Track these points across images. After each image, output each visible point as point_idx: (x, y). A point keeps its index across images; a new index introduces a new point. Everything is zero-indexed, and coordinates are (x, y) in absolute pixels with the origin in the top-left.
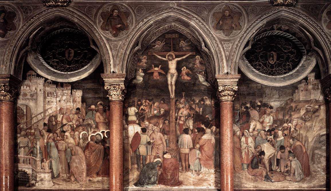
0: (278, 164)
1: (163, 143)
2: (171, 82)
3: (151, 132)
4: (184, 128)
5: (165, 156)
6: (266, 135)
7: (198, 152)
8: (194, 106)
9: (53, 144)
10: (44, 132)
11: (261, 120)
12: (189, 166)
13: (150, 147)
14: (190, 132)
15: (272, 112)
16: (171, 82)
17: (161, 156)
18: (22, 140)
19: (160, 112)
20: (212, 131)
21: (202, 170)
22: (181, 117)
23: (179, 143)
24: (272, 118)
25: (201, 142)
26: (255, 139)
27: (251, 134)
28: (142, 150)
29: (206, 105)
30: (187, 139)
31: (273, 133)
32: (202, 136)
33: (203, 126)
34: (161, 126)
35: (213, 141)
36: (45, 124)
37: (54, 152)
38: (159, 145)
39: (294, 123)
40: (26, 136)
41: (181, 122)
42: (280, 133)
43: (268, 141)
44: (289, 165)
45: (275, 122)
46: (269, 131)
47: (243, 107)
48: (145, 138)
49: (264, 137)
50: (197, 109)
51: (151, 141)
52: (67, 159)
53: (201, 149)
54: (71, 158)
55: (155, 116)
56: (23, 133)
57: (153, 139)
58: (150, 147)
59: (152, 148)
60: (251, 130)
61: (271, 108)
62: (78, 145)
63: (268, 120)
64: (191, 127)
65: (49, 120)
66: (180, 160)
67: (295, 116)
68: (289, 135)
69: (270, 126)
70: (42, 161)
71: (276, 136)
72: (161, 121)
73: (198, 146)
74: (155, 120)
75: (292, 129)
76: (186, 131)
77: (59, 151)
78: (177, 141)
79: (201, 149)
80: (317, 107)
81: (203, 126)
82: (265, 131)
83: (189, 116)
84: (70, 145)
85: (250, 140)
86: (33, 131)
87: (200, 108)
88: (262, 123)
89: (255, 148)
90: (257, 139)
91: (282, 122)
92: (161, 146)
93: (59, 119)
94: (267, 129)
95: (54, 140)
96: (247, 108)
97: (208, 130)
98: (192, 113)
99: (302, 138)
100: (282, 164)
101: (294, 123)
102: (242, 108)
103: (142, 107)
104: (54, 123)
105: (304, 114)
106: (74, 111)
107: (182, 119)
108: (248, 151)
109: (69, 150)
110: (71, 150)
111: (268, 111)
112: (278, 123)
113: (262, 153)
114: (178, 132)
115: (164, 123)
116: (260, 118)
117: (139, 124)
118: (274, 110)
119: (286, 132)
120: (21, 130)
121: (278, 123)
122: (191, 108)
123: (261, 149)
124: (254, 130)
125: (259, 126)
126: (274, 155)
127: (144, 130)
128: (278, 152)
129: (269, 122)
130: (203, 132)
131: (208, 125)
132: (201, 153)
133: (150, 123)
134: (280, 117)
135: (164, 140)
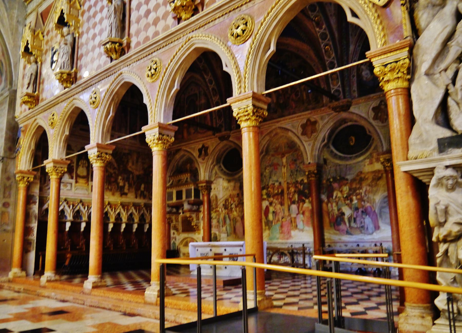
0: (355, 221)
1: (281, 211)
2: (284, 172)
3: (274, 205)
4: (293, 200)
5: (283, 220)
6: (345, 200)
7: (302, 216)
8: (297, 185)
9: (227, 216)
10: (223, 209)
11: (341, 190)
12: (297, 226)
13: (274, 214)
14: (296, 203)
15: (347, 183)
16: (284, 172)
17: (280, 219)
18: (214, 215)
19: (278, 191)
20: (309, 201)
21: (305, 229)
22: (290, 193)
23: (290, 210)
24: (348, 187)
25: (304, 209)
26: (337, 204)
27: (334, 201)
28: (271, 217)
29: (305, 183)
30: (294, 207)
31: (349, 198)
32: (303, 204)
33: (304, 198)
34: (280, 200)
35: (310, 208)
36: (223, 205)
37: (228, 221)
38: (279, 213)
39: (364, 189)
40: (216, 212)
41: (291, 197)
42: (354, 198)
43: (347, 205)
44: (363, 221)
45: (350, 189)
46: (346, 197)
47: (328, 182)
48: (271, 209)
49: (343, 202)
50: (299, 187)
51: (275, 211)
52: (234, 225)
53: (303, 213)
54: (236, 224)
55: (277, 194)
56: (214, 210)
57: (276, 209)
58: (274, 214)
59: (276, 215)
60: (334, 197)
61: (347, 180)
62: (239, 216)
63: (346, 189)
64: (297, 199)
65: (226, 202)
66: (291, 222)
67: (364, 184)
68: (361, 200)
69: (347, 193)
70: (223, 226)
71: (352, 200)
72: (279, 197)
73: (301, 212)
74: (276, 197)
75: (363, 194)
76: (293, 203)
77: (230, 220)
78: (289, 210)
79: (303, 213)
80: (380, 175)
81: (304, 198)
82: (343, 197)
83: (295, 192)
84: (235, 216)
85: (334, 204)
86: (218, 209)
87: (301, 185)
88: (341, 192)
89: (339, 210)
90: (339, 203)
91: (355, 190)
92: (280, 214)
93: (230, 201)
94: (345, 196)
95: (228, 214)
96: (330, 182)
97: (307, 201)
98: (297, 190)
99: (371, 201)
100: (358, 222)
101: (364, 189)
102: (327, 182)
103: (269, 189)
104: (227, 203)
105: (371, 182)
106: (236, 196)
107: (291, 194)
108: (333, 213)
109: (234, 219)
110: (236, 219)
111: (345, 182)
112: (353, 190)
113: (343, 214)
114: (289, 203)
115: (281, 198)
116: (340, 187)
117: (268, 200)
118: (349, 181)
119: (359, 197)
120: (213, 209)
121: (353, 190)
122: (296, 187)
123: (342, 211)
124: (336, 197)
125: (339, 195)
126: (351, 215)
127: (271, 204)
128: (354, 213)
129: (346, 191)
130: (304, 202)
131: (307, 197)
132: (304, 216)
133: (273, 199)
134: (354, 186)
135: (282, 209)
